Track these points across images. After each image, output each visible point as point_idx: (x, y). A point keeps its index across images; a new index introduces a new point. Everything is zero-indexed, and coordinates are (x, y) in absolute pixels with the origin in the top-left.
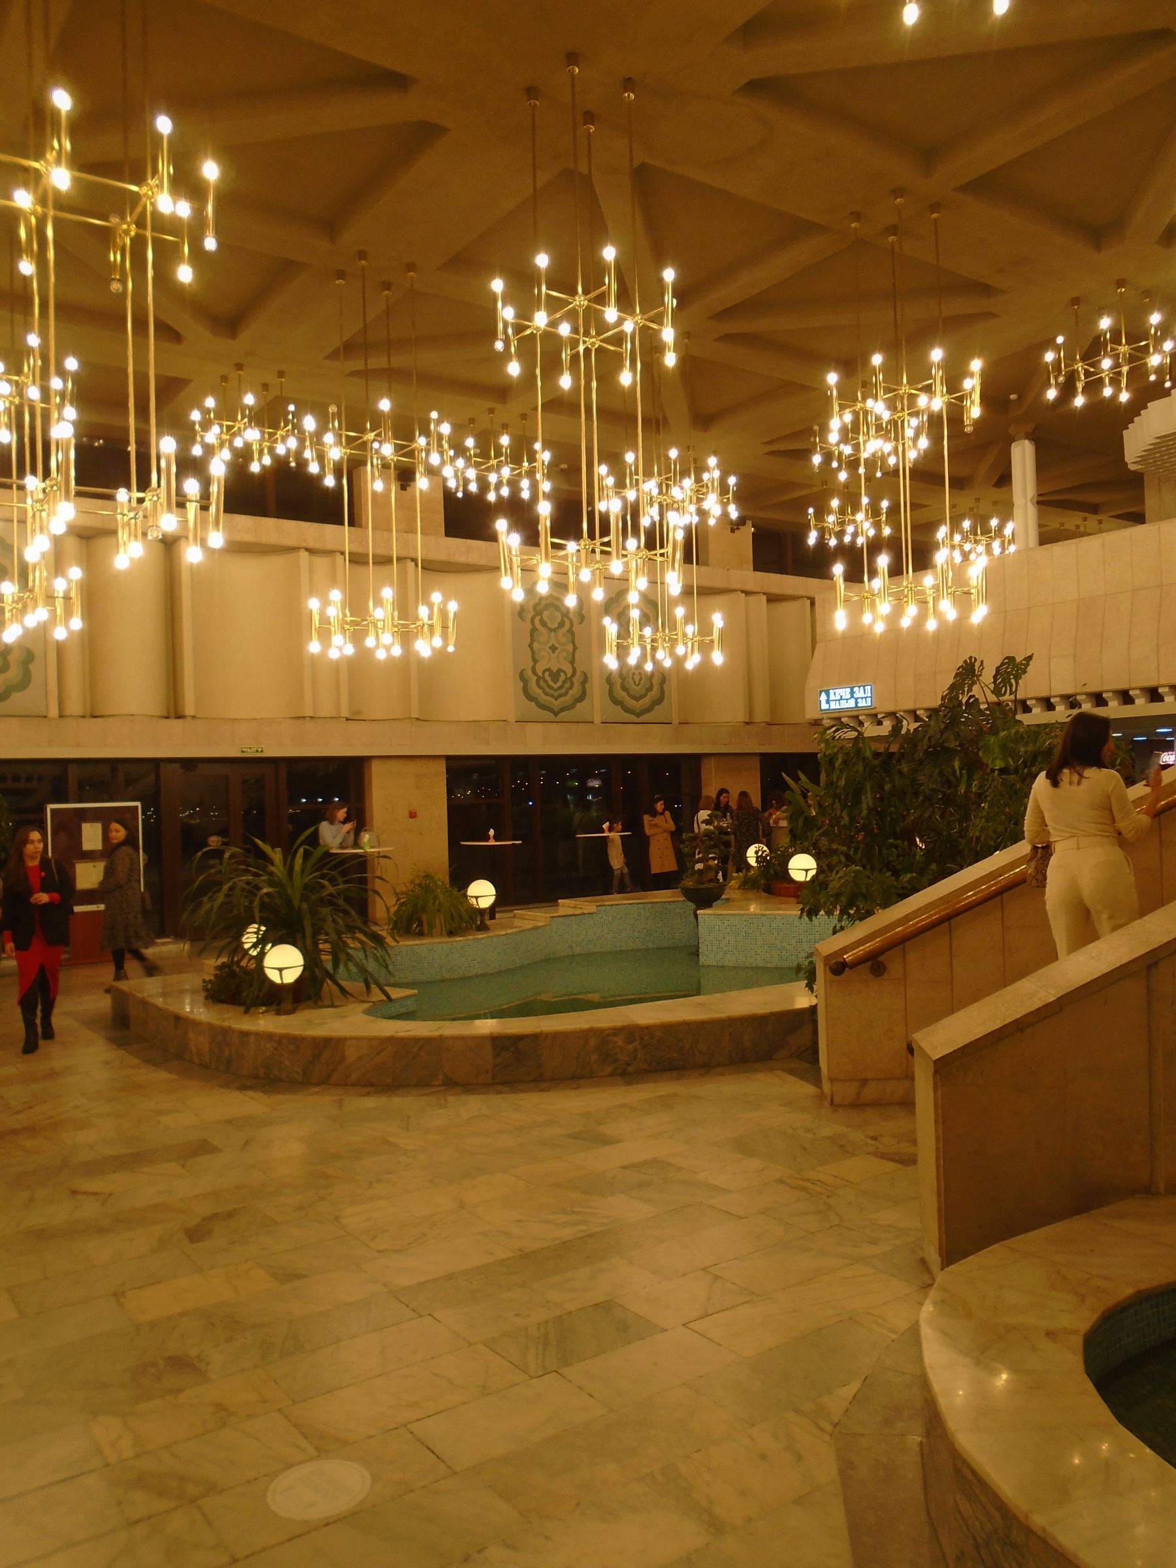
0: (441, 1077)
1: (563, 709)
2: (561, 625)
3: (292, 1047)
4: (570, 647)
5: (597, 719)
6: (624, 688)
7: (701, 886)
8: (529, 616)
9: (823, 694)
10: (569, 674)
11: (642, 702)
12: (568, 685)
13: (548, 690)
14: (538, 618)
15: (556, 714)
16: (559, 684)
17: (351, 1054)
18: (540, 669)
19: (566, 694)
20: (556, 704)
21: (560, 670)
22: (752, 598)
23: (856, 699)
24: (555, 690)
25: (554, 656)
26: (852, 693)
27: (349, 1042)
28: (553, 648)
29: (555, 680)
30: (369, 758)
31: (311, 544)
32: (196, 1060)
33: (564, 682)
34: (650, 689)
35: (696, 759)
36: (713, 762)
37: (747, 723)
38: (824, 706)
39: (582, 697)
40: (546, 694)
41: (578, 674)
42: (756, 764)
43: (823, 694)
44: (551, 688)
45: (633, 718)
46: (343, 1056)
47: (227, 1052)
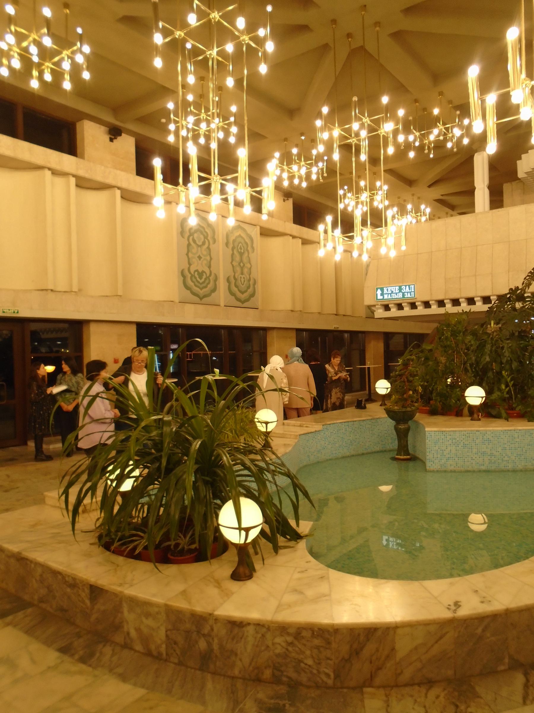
0: (507, 660)
1: (205, 296)
2: (204, 243)
3: (317, 642)
4: (208, 258)
5: (222, 304)
7: (404, 410)
8: (186, 235)
9: (379, 290)
10: (208, 276)
11: (245, 295)
12: (207, 281)
13: (197, 283)
14: (191, 237)
15: (201, 299)
16: (203, 280)
17: (403, 646)
18: (192, 270)
19: (206, 287)
20: (201, 292)
21: (203, 272)
22: (295, 240)
23: (403, 294)
24: (201, 284)
25: (200, 262)
26: (400, 290)
27: (399, 631)
28: (200, 258)
29: (201, 278)
30: (88, 322)
31: (53, 166)
32: (138, 647)
33: (205, 279)
34: (249, 287)
35: (265, 329)
36: (275, 333)
37: (292, 311)
38: (379, 297)
39: (214, 290)
40: (196, 286)
41: (213, 275)
42: (294, 334)
43: (379, 290)
44: (198, 282)
45: (239, 304)
46: (393, 649)
47: (202, 645)
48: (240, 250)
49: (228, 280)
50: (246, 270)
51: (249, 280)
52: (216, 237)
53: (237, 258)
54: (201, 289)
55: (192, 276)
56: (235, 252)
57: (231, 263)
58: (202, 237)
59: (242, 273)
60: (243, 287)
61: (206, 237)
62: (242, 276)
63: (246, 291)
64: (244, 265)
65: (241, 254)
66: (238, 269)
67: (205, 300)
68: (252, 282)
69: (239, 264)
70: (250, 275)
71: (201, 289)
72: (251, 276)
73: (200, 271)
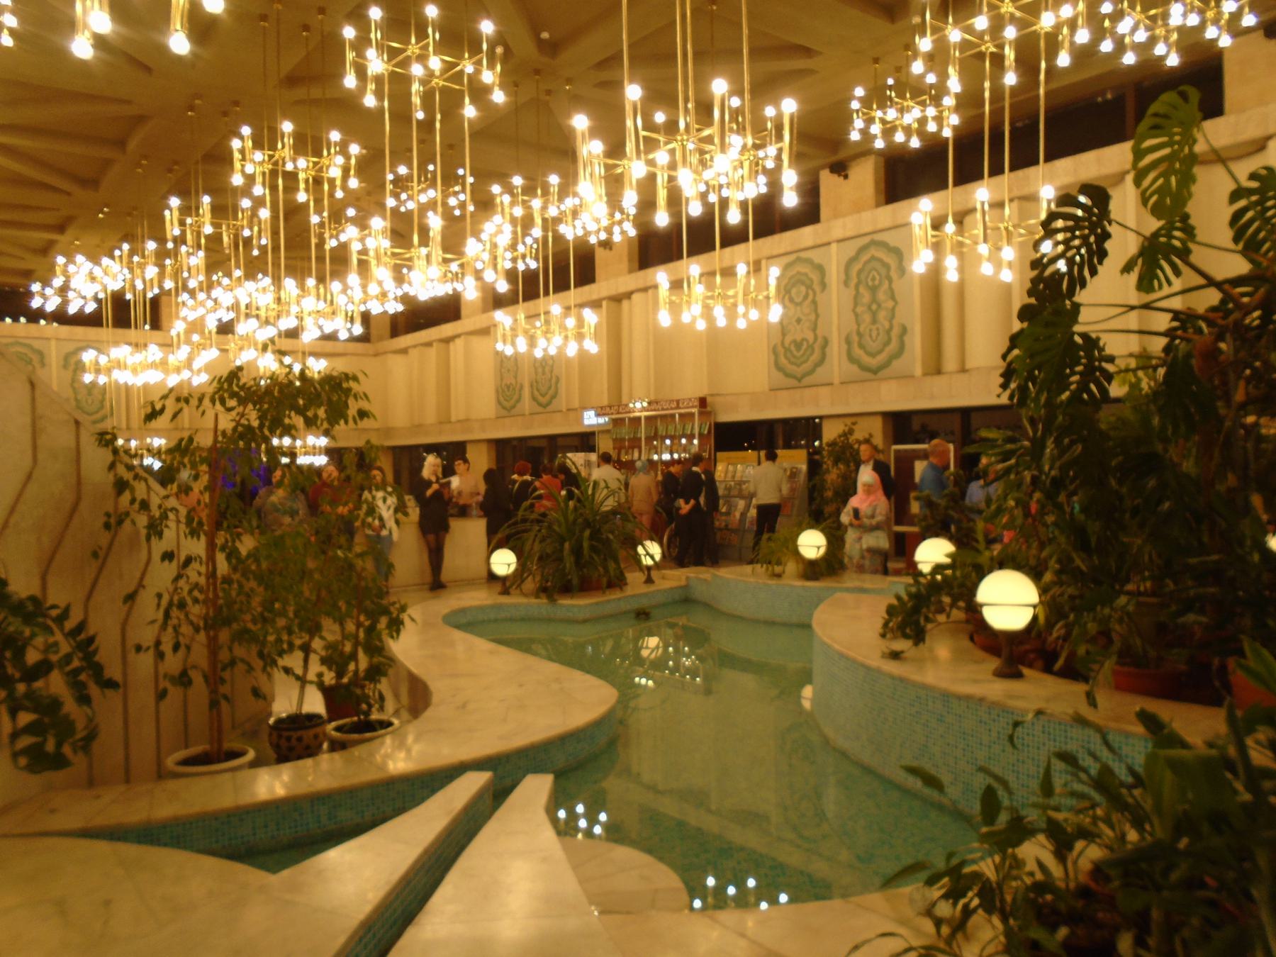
2: (806, 297)
4: (813, 317)
5: (836, 381)
6: (861, 346)
15: (799, 380)
18: (788, 340)
19: (805, 362)
20: (799, 371)
21: (803, 340)
39: (821, 361)
40: (792, 363)
44: (794, 356)
48: (870, 283)
49: (848, 341)
50: (882, 315)
51: (891, 328)
52: (826, 280)
53: (866, 297)
54: (798, 366)
55: (787, 350)
56: (862, 290)
57: (854, 310)
58: (803, 289)
59: (874, 321)
60: (873, 346)
61: (809, 287)
62: (874, 327)
63: (881, 351)
64: (879, 306)
65: (874, 290)
66: (867, 317)
67: (806, 381)
68: (895, 332)
69: (869, 308)
70: (893, 316)
71: (798, 366)
72: (895, 322)
73: (799, 339)
